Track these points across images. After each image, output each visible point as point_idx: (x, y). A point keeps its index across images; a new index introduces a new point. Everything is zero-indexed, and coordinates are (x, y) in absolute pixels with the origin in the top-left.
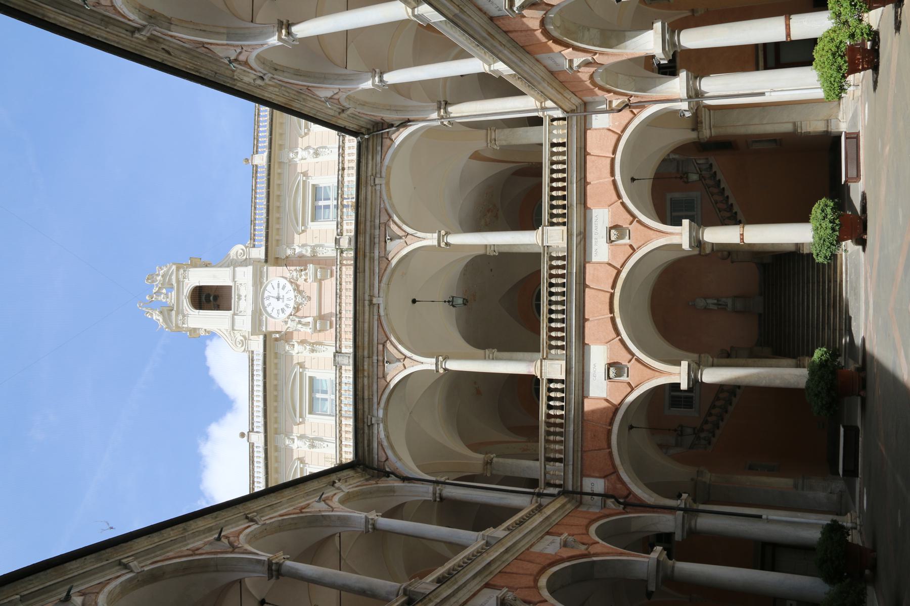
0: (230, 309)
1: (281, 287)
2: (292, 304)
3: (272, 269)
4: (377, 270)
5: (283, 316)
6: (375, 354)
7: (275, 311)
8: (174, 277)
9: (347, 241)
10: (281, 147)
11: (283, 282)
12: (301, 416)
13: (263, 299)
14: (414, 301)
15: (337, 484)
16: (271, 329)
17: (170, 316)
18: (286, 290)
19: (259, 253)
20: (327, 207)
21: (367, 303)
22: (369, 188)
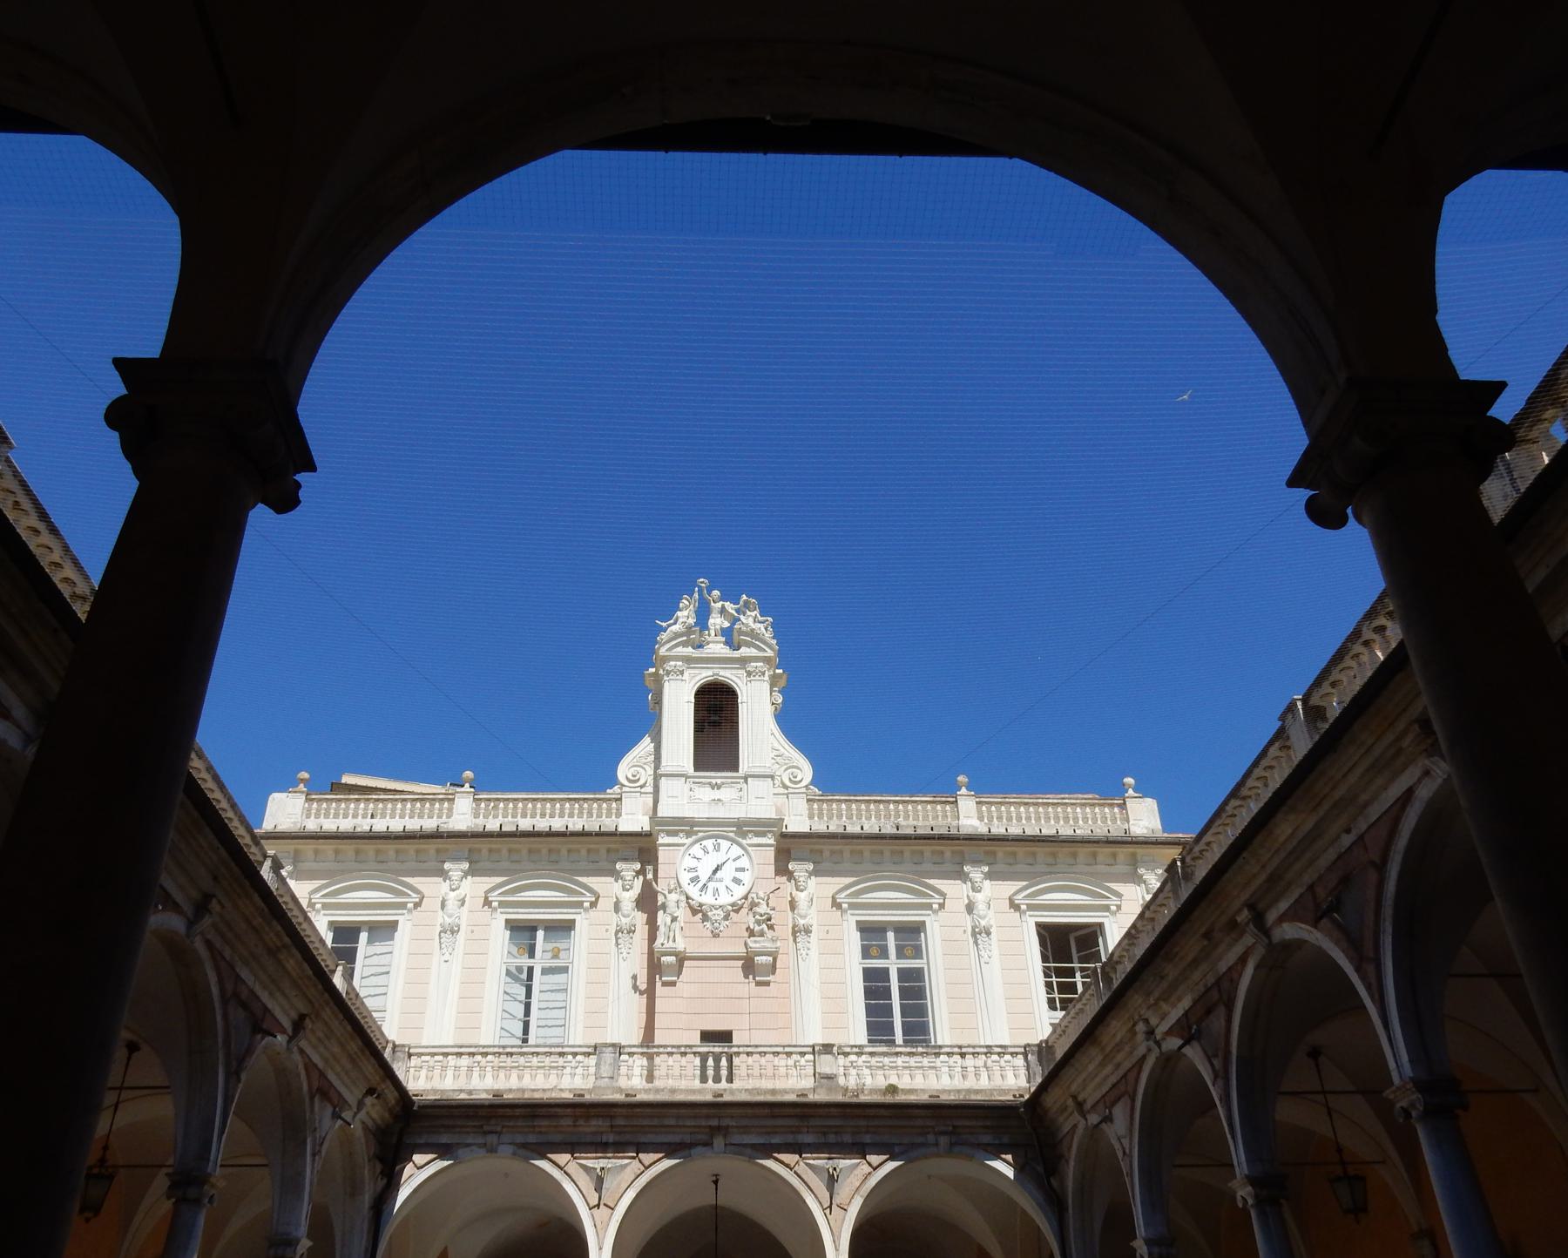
0: (697, 768)
1: (739, 875)
2: (707, 899)
3: (770, 854)
4: (774, 1141)
5: (685, 878)
6: (617, 1138)
7: (693, 863)
8: (753, 652)
9: (827, 1070)
10: (989, 859)
11: (746, 877)
12: (502, 904)
13: (717, 837)
14: (716, 1182)
15: (369, 1100)
16: (663, 855)
17: (684, 644)
18: (733, 886)
19: (798, 822)
20: (884, 953)
21: (714, 1123)
22: (929, 1123)
